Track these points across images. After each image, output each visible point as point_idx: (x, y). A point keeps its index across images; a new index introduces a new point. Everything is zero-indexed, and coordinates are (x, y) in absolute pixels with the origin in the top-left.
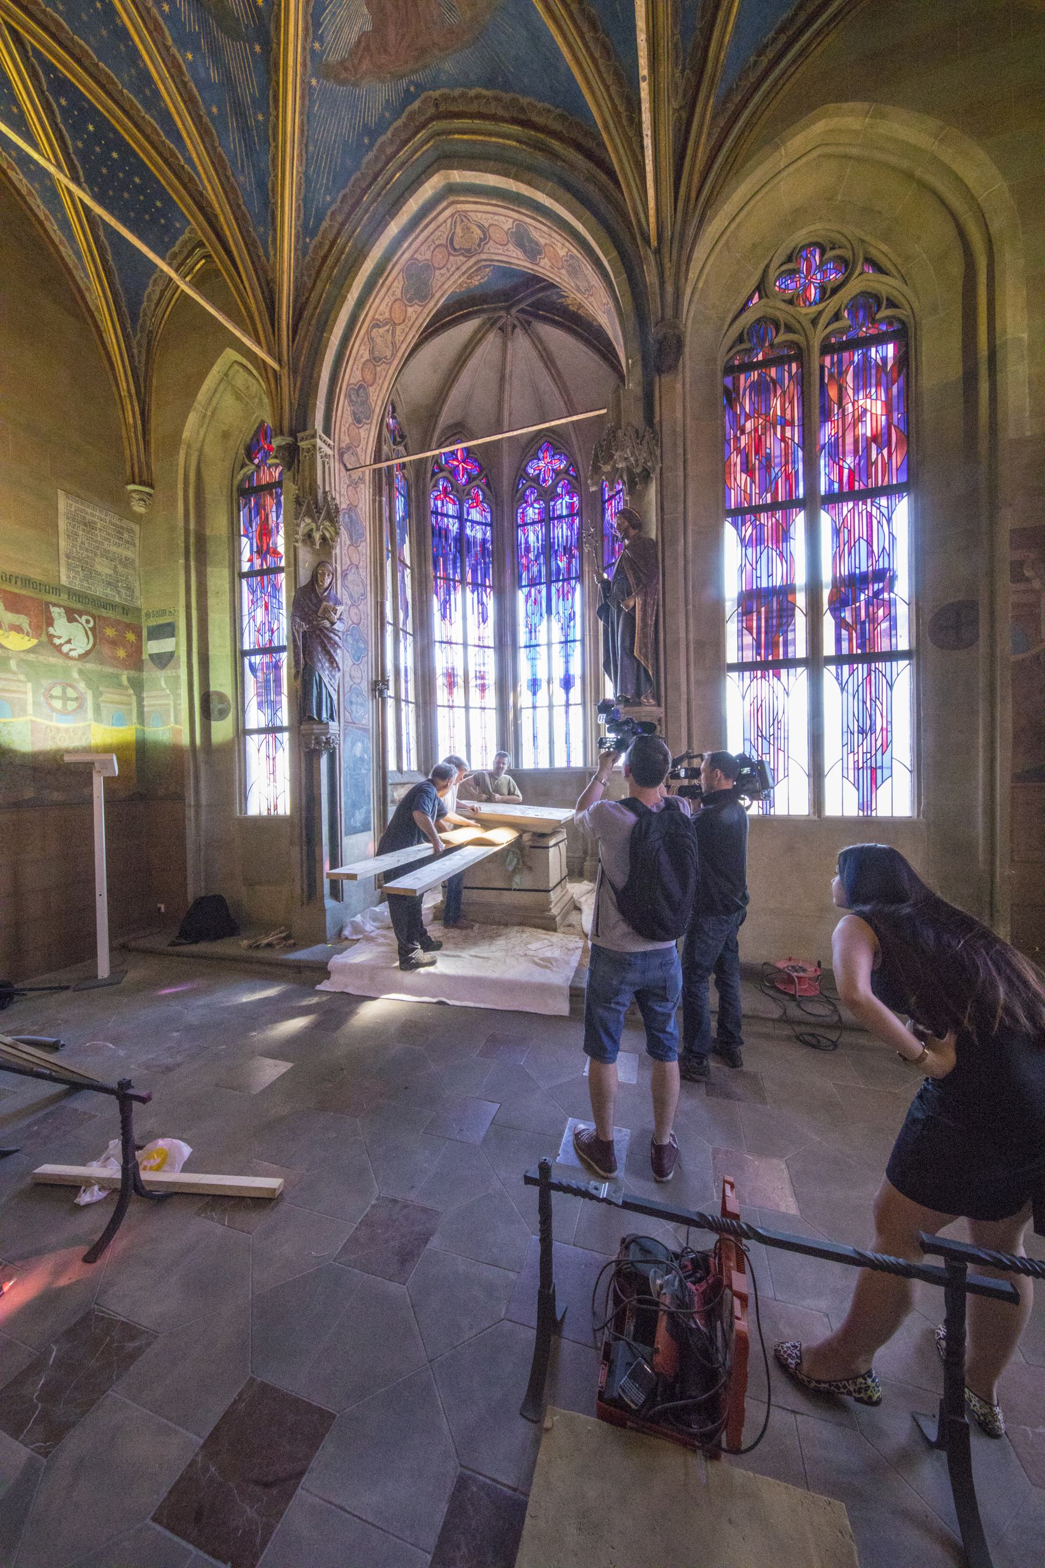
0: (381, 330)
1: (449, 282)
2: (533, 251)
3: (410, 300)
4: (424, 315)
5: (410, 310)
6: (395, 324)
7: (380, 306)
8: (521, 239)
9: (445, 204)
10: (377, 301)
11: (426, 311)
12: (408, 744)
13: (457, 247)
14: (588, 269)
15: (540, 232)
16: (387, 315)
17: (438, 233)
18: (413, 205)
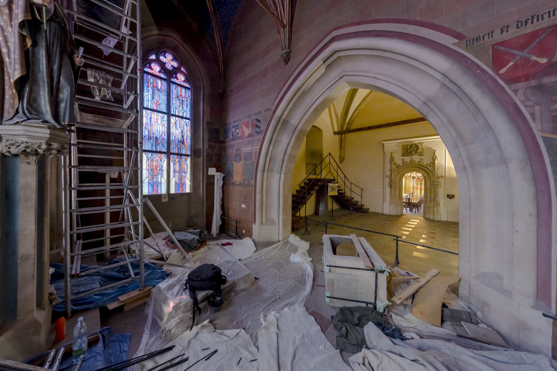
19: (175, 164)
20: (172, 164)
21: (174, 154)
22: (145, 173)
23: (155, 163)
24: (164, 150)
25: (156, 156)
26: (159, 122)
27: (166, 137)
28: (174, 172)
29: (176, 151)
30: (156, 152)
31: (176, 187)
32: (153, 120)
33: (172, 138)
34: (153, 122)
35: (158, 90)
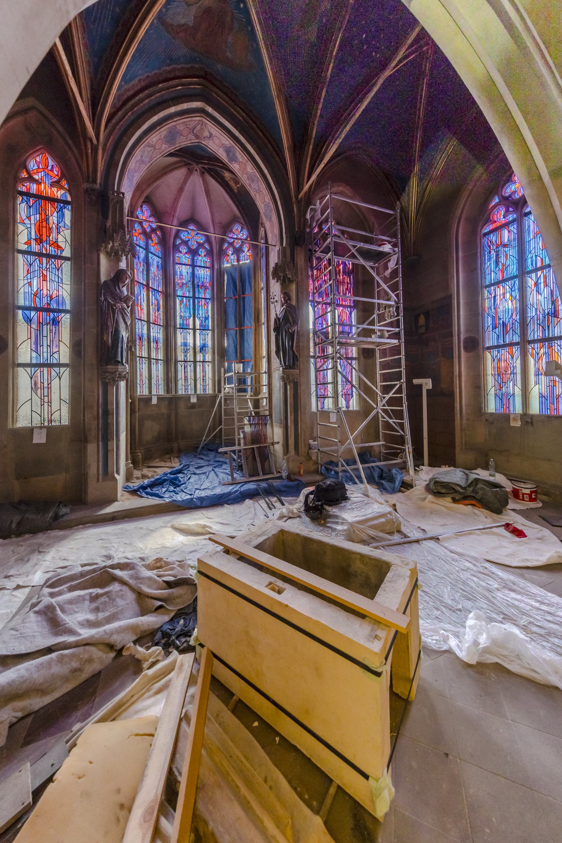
0: (149, 149)
1: (183, 142)
2: (233, 159)
3: (166, 142)
4: (167, 150)
5: (164, 146)
6: (155, 149)
7: (154, 138)
8: (228, 151)
9: (199, 115)
10: (154, 135)
11: (169, 149)
12: (158, 380)
13: (194, 132)
14: (263, 186)
15: (240, 155)
16: (154, 143)
17: (190, 123)
18: (185, 106)
19: (537, 361)
20: (531, 361)
21: (534, 341)
22: (490, 381)
23: (503, 364)
24: (516, 339)
25: (504, 353)
26: (508, 295)
27: (518, 317)
28: (537, 374)
29: (539, 334)
30: (504, 346)
31: (541, 403)
32: (498, 298)
33: (531, 313)
34: (498, 302)
35: (505, 246)
